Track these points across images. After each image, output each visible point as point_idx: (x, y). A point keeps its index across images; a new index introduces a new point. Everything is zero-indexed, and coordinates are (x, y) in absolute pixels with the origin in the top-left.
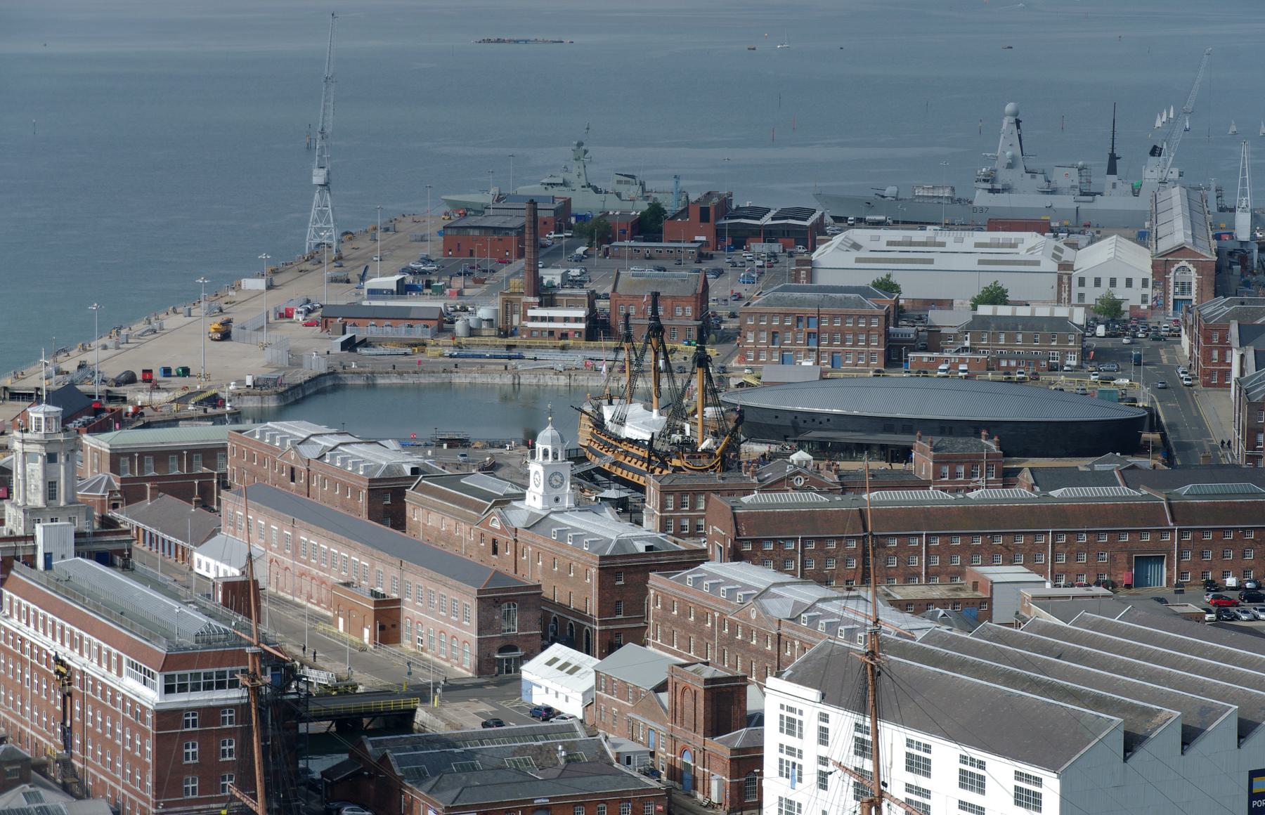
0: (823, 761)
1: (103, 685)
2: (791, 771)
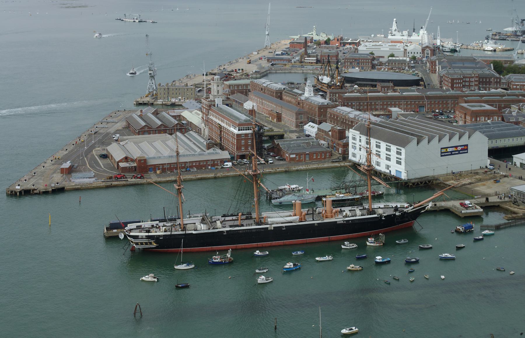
0: (360, 145)
1: (227, 129)
2: (354, 148)
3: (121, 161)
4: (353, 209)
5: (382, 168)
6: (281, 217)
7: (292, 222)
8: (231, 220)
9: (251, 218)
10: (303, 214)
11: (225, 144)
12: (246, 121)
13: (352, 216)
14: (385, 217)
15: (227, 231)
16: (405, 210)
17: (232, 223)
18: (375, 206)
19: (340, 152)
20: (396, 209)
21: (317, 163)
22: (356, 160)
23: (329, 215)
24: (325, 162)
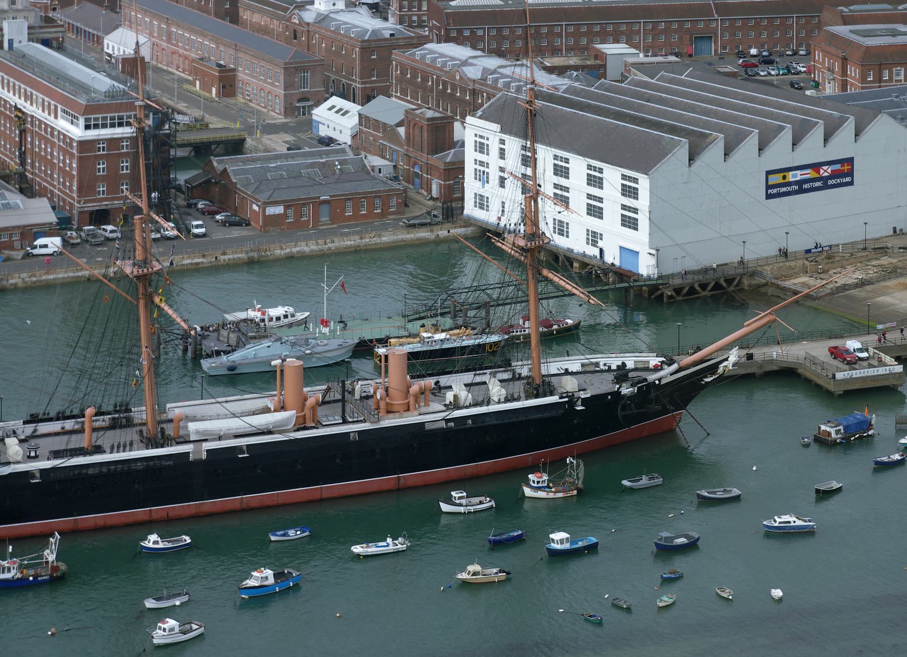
0: (502, 170)
1: (46, 125)
2: (482, 177)
4: (478, 379)
6: (234, 415)
7: (270, 432)
8: (57, 434)
9: (129, 423)
10: (311, 401)
12: (111, 94)
13: (476, 404)
14: (585, 401)
15: (42, 471)
16: (652, 377)
17: (60, 443)
18: (553, 367)
19: (435, 193)
20: (622, 374)
21: (356, 233)
22: (489, 217)
23: (398, 401)
24: (384, 228)
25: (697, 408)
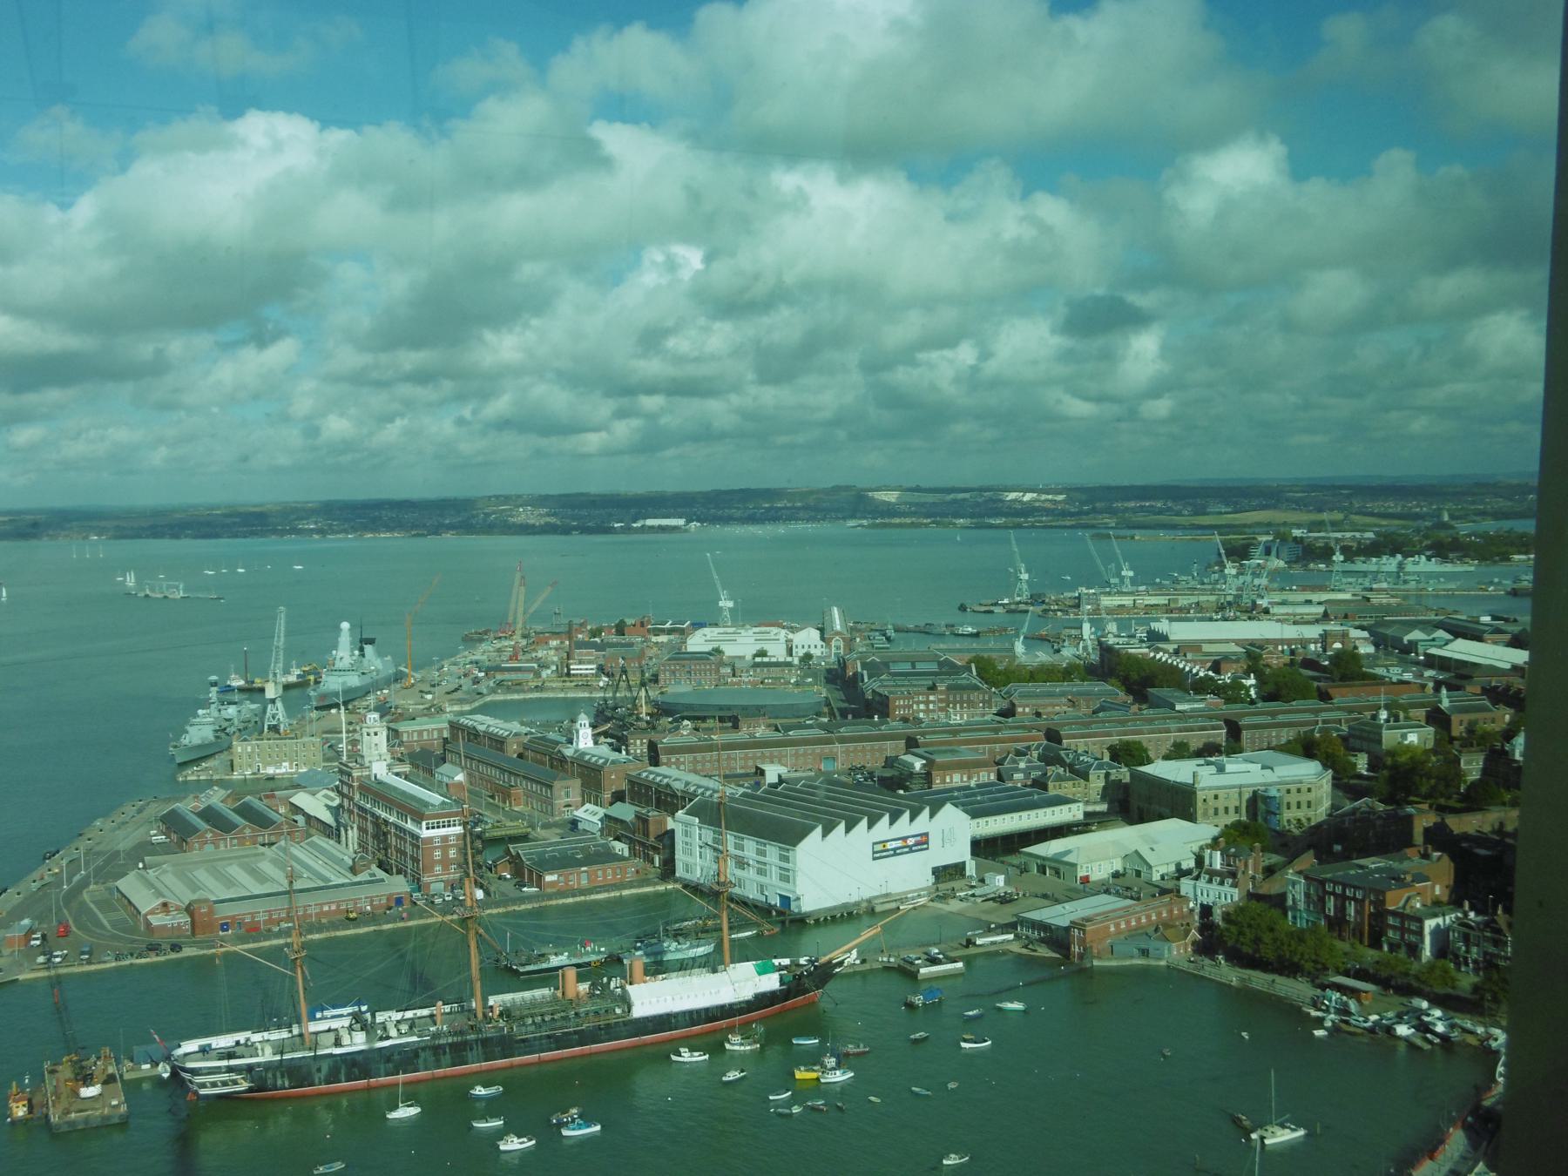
3: (152, 912)
5: (752, 894)
11: (393, 858)
25: (831, 986)
